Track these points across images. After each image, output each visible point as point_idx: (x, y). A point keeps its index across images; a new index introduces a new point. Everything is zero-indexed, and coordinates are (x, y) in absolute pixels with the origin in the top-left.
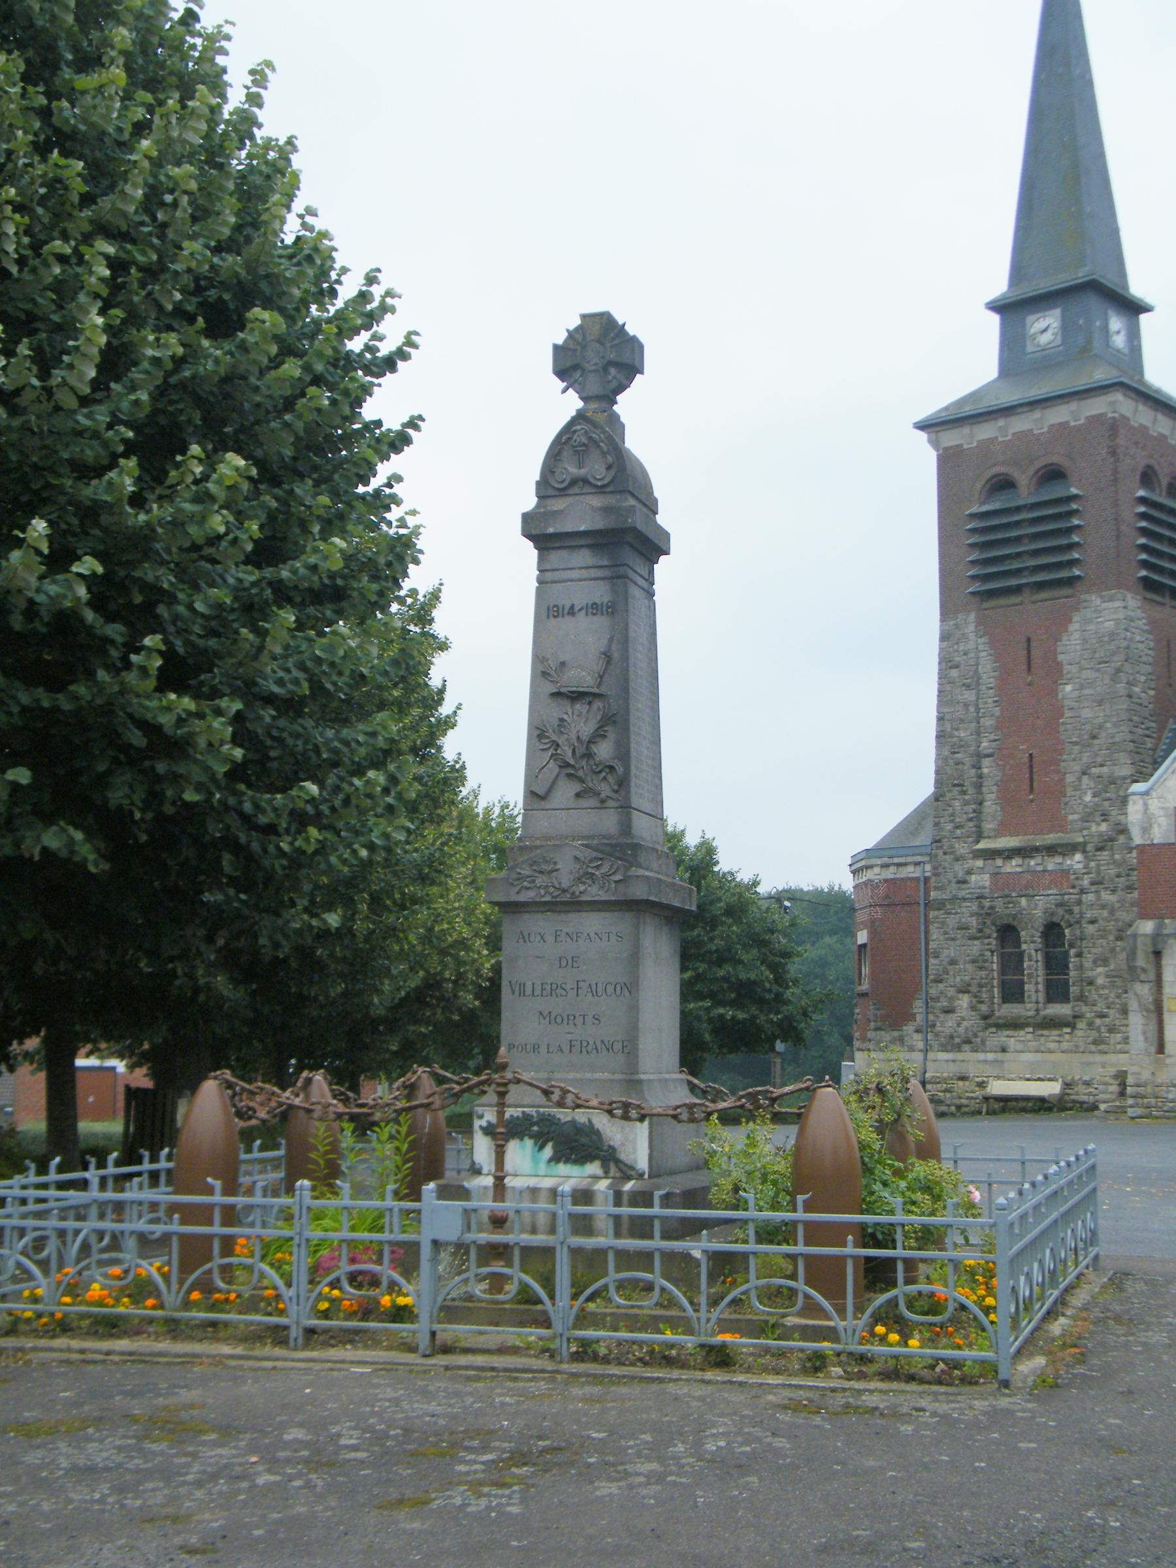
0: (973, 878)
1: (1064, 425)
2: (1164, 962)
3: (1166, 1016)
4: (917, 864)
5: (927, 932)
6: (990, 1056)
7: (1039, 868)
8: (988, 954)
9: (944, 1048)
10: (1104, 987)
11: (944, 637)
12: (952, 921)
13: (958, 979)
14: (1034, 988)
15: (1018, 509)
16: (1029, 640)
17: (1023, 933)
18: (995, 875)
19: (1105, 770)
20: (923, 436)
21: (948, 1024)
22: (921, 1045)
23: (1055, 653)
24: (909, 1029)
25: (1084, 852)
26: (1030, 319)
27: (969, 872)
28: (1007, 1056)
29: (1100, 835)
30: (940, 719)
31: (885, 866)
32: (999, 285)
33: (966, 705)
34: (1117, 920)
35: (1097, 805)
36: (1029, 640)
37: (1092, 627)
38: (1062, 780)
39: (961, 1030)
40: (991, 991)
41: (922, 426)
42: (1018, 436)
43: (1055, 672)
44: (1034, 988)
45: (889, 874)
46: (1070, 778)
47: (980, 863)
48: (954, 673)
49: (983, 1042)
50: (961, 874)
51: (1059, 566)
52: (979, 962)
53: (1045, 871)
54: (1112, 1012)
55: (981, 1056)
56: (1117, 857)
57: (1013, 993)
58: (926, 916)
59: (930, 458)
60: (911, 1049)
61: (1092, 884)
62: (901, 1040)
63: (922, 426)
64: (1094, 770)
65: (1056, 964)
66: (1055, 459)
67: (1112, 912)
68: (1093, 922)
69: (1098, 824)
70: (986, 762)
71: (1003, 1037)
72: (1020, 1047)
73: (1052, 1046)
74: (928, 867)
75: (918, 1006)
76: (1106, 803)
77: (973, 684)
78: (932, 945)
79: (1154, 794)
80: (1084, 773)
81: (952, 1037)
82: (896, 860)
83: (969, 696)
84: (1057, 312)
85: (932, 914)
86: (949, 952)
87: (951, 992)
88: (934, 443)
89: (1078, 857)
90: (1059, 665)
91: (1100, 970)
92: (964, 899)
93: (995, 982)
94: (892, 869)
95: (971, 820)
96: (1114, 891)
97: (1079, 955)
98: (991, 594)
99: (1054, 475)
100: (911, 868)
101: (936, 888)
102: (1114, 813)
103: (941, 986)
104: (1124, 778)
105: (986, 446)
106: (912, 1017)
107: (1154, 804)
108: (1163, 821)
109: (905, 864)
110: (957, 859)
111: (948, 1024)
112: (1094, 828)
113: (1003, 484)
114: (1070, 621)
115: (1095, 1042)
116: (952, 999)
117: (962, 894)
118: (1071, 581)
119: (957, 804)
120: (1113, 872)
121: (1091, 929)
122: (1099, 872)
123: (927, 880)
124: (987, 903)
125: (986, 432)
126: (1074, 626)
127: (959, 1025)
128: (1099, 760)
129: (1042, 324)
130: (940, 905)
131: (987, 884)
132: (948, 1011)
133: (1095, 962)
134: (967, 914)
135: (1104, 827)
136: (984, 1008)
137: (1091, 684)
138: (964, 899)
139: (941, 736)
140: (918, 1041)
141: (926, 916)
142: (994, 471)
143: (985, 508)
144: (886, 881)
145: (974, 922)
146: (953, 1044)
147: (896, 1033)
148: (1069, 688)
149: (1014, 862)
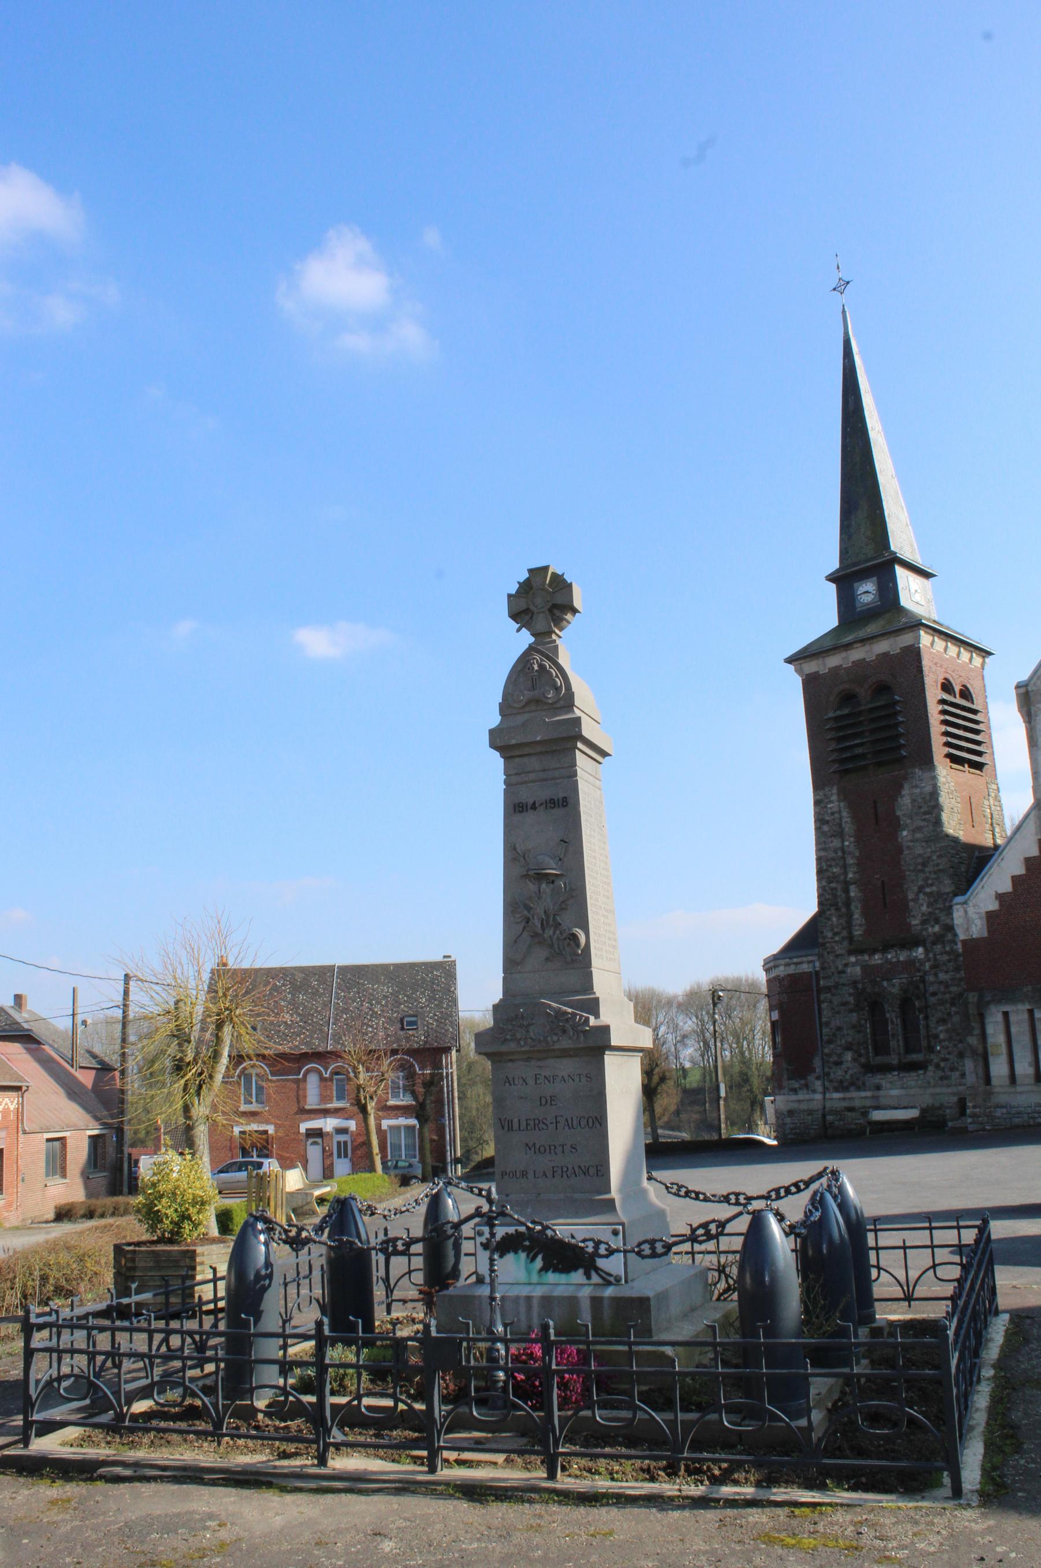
0: (849, 970)
1: (885, 655)
2: (987, 1021)
3: (991, 1059)
5: (820, 1010)
6: (869, 1094)
7: (894, 960)
8: (863, 1022)
9: (836, 1090)
10: (944, 1041)
11: (817, 803)
12: (836, 1000)
13: (843, 1042)
14: (897, 1044)
15: (860, 713)
16: (875, 802)
17: (886, 1006)
18: (865, 968)
19: (934, 888)
20: (791, 667)
21: (838, 1073)
22: (820, 1089)
23: (894, 811)
24: (811, 1078)
25: (924, 947)
26: (856, 585)
27: (846, 965)
28: (882, 1093)
29: (935, 934)
31: (787, 965)
32: (833, 564)
33: (835, 851)
34: (950, 992)
35: (930, 913)
36: (875, 802)
37: (917, 791)
39: (848, 1077)
40: (867, 1048)
41: (790, 660)
42: (857, 664)
43: (895, 825)
44: (897, 1044)
45: (791, 970)
46: (911, 896)
47: (853, 959)
49: (864, 1084)
50: (840, 968)
52: (857, 1028)
53: (899, 961)
54: (950, 1057)
55: (863, 1094)
56: (947, 949)
57: (881, 1047)
58: (818, 998)
59: (797, 682)
60: (814, 1091)
61: (932, 967)
62: (807, 1086)
63: (790, 660)
64: (928, 890)
65: (909, 1025)
67: (947, 986)
68: (934, 994)
69: (933, 926)
70: (852, 888)
71: (877, 1079)
72: (888, 1085)
73: (913, 1083)
74: (817, 964)
75: (817, 1062)
76: (937, 911)
77: (840, 834)
78: (824, 1020)
79: (971, 904)
80: (920, 892)
81: (841, 1082)
82: (795, 960)
83: (836, 843)
84: (875, 579)
85: (822, 997)
86: (836, 1022)
87: (839, 1051)
88: (799, 671)
89: (921, 950)
90: (898, 817)
91: (941, 1028)
94: (793, 967)
95: (843, 929)
96: (947, 972)
97: (926, 1018)
98: (846, 772)
99: (883, 689)
101: (824, 978)
102: (942, 918)
103: (832, 1046)
104: (948, 893)
105: (835, 671)
106: (813, 1070)
107: (971, 910)
108: (978, 922)
109: (801, 963)
110: (837, 956)
111: (838, 1073)
112: (930, 929)
113: (848, 698)
114: (901, 787)
115: (942, 1078)
116: (840, 1055)
117: (842, 981)
118: (901, 760)
119: (834, 919)
120: (945, 958)
121: (933, 1000)
122: (935, 959)
123: (817, 973)
125: (834, 661)
126: (905, 792)
127: (846, 1072)
128: (930, 882)
130: (828, 989)
132: (839, 1063)
133: (937, 1022)
134: (847, 995)
135: (937, 928)
136: (863, 1060)
137: (919, 829)
138: (844, 985)
139: (820, 872)
140: (818, 1084)
141: (818, 998)
142: (841, 687)
143: (839, 713)
144: (788, 975)
145: (851, 999)
146: (842, 1086)
147: (803, 1082)
148: (905, 833)
149: (876, 957)
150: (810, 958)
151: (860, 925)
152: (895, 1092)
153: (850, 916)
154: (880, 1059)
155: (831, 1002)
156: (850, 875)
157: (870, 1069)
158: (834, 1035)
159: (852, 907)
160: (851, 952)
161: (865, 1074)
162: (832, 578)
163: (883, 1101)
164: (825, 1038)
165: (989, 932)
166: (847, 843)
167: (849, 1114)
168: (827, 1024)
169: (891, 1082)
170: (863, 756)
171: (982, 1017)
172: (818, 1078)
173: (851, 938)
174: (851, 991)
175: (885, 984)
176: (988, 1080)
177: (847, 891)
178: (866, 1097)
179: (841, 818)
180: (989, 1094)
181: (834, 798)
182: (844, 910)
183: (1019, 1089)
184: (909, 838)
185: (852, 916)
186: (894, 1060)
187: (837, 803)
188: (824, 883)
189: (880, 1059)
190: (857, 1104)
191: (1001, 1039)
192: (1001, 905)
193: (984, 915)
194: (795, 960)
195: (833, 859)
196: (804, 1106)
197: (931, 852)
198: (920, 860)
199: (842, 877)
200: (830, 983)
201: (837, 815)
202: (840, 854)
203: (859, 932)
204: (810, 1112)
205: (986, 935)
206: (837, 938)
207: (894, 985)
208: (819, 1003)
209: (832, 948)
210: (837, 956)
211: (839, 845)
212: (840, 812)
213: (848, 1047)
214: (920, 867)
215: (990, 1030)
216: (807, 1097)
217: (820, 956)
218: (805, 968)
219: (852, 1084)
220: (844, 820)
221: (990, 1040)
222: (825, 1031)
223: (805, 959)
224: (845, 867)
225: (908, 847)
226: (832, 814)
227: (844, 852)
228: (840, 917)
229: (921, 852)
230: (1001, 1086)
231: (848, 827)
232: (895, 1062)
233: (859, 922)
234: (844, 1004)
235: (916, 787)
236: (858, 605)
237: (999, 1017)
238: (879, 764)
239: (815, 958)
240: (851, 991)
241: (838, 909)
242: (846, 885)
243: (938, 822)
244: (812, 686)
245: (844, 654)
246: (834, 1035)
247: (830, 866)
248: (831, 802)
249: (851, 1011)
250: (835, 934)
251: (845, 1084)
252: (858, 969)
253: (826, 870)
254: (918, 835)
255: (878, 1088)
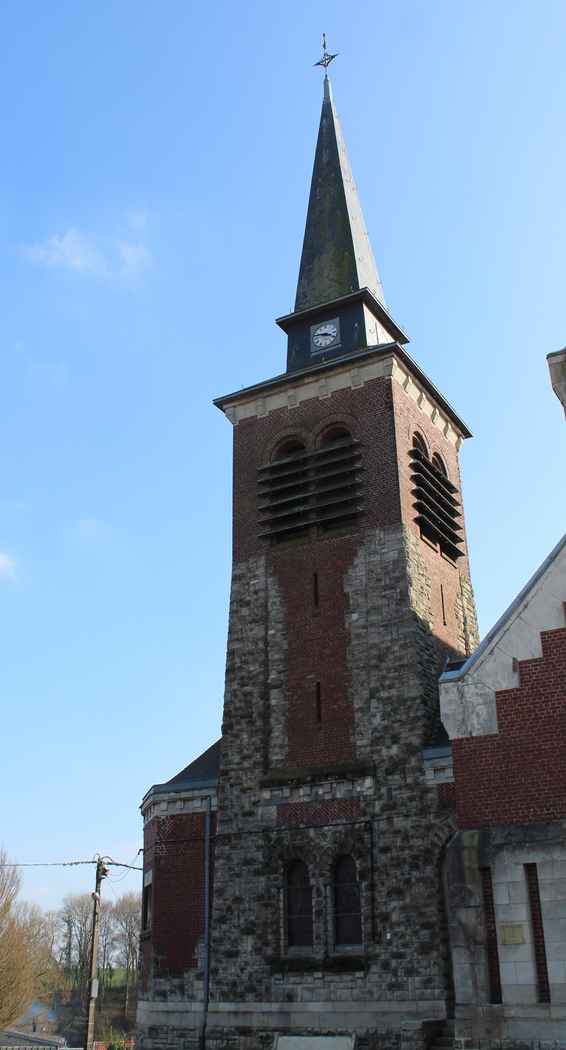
0: (260, 811)
1: (346, 391)
2: (494, 881)
3: (501, 951)
4: (203, 798)
5: (212, 869)
6: (275, 1007)
7: (328, 797)
8: (274, 890)
9: (225, 997)
10: (399, 924)
11: (235, 579)
12: (237, 856)
13: (242, 920)
14: (323, 927)
15: (305, 460)
16: (316, 576)
17: (311, 867)
18: (283, 808)
19: (394, 692)
21: (230, 971)
22: (201, 995)
23: (342, 586)
24: (190, 975)
25: (374, 776)
26: (312, 328)
27: (256, 804)
28: (294, 1006)
29: (391, 758)
30: (231, 654)
31: (172, 802)
32: (288, 308)
34: (410, 848)
35: (385, 727)
36: (316, 576)
38: (349, 706)
39: (245, 977)
40: (276, 932)
41: (220, 403)
43: (342, 604)
44: (323, 927)
45: (177, 809)
46: (357, 704)
47: (266, 795)
48: (245, 611)
49: (268, 989)
50: (247, 807)
51: (345, 505)
52: (264, 899)
53: (334, 799)
54: (408, 951)
55: (265, 1007)
56: (409, 780)
57: (298, 933)
58: (211, 852)
60: (192, 998)
61: (384, 809)
62: (181, 988)
63: (220, 403)
64: (384, 694)
65: (345, 902)
66: (339, 418)
67: (406, 837)
68: (385, 850)
69: (389, 747)
71: (290, 983)
72: (306, 995)
73: (346, 993)
74: (214, 801)
75: (201, 951)
76: (396, 725)
77: (265, 620)
78: (216, 885)
80: (372, 696)
81: (234, 984)
82: (183, 795)
83: (257, 631)
84: (337, 320)
85: (217, 851)
86: (233, 890)
89: (369, 782)
90: (347, 596)
91: (394, 904)
92: (250, 833)
93: (281, 922)
94: (179, 804)
95: (257, 750)
96: (407, 816)
97: (372, 887)
98: (280, 537)
99: (337, 432)
100: (197, 803)
101: (222, 822)
102: (403, 735)
103: (224, 927)
104: (414, 699)
105: (277, 415)
106: (194, 964)
107: (470, 691)
108: (482, 710)
109: (192, 799)
110: (244, 791)
111: (230, 971)
112: (384, 751)
113: (292, 446)
114: (355, 554)
115: (392, 987)
117: (248, 827)
119: (245, 736)
120: (405, 794)
121: (383, 859)
122: (390, 797)
123: (213, 815)
124: (274, 835)
127: (242, 970)
128: (387, 683)
129: (324, 330)
130: (227, 838)
131: (275, 816)
132: (232, 955)
133: (389, 894)
135: (394, 750)
136: (269, 951)
137: (376, 609)
138: (250, 833)
140: (199, 987)
141: (211, 852)
142: (284, 433)
143: (276, 463)
144: (172, 817)
145: (259, 856)
146: (234, 993)
147: (176, 981)
148: (355, 616)
149: (302, 792)
150: (205, 792)
151: (281, 747)
152: (314, 1007)
153: (267, 733)
154: (295, 952)
155: (229, 858)
156: (273, 676)
157: (278, 965)
158: (229, 909)
159: (272, 721)
160: (263, 785)
161: (271, 973)
162: (284, 323)
163: (297, 1021)
164: (215, 914)
165: (500, 726)
166: (272, 632)
167: (242, 1038)
168: (221, 892)
169: (311, 990)
170: (306, 514)
171: (486, 873)
172: (199, 977)
173: (266, 764)
174: (261, 842)
175: (312, 832)
176: (495, 992)
177: (265, 697)
178: (270, 1013)
179: (267, 598)
180: (498, 1020)
181: (260, 571)
182: (259, 723)
183: (557, 1012)
184: (361, 622)
185: (270, 732)
186: (317, 953)
187: (263, 578)
188: (235, 686)
189: (295, 952)
190: (255, 1022)
191: (522, 914)
192: (522, 681)
193: (492, 697)
194: (183, 795)
195: (251, 653)
196: (174, 1021)
197: (392, 640)
198: (375, 652)
199: (261, 678)
200: (231, 829)
201: (262, 594)
202: (261, 645)
203: (279, 757)
204: (183, 1032)
205: (495, 731)
206: (246, 764)
207: (325, 836)
208: (212, 859)
209: (238, 778)
210: (244, 791)
211: (262, 633)
212: (266, 589)
213: (248, 931)
214: (374, 662)
215: (501, 897)
216: (180, 1006)
217: (220, 789)
218: (197, 806)
219: (251, 989)
220: (270, 601)
221: (500, 916)
222: (217, 902)
223: (197, 793)
224: (266, 664)
225: (358, 636)
226: (256, 592)
227: (266, 644)
228: (253, 733)
229: (377, 640)
230: (522, 1006)
231: (276, 609)
232: (319, 956)
233: (280, 742)
234: (248, 862)
235: (375, 553)
236: (313, 349)
237: (520, 875)
238: (326, 526)
239: (213, 792)
240: (261, 842)
241: (251, 723)
242: (266, 688)
243: (404, 598)
244: (244, 434)
245: (291, 392)
246: (229, 909)
247: (246, 663)
248: (255, 577)
249: (258, 873)
250: (244, 758)
251: (240, 989)
252: (273, 809)
253: (241, 668)
254: (374, 618)
255: (290, 998)
